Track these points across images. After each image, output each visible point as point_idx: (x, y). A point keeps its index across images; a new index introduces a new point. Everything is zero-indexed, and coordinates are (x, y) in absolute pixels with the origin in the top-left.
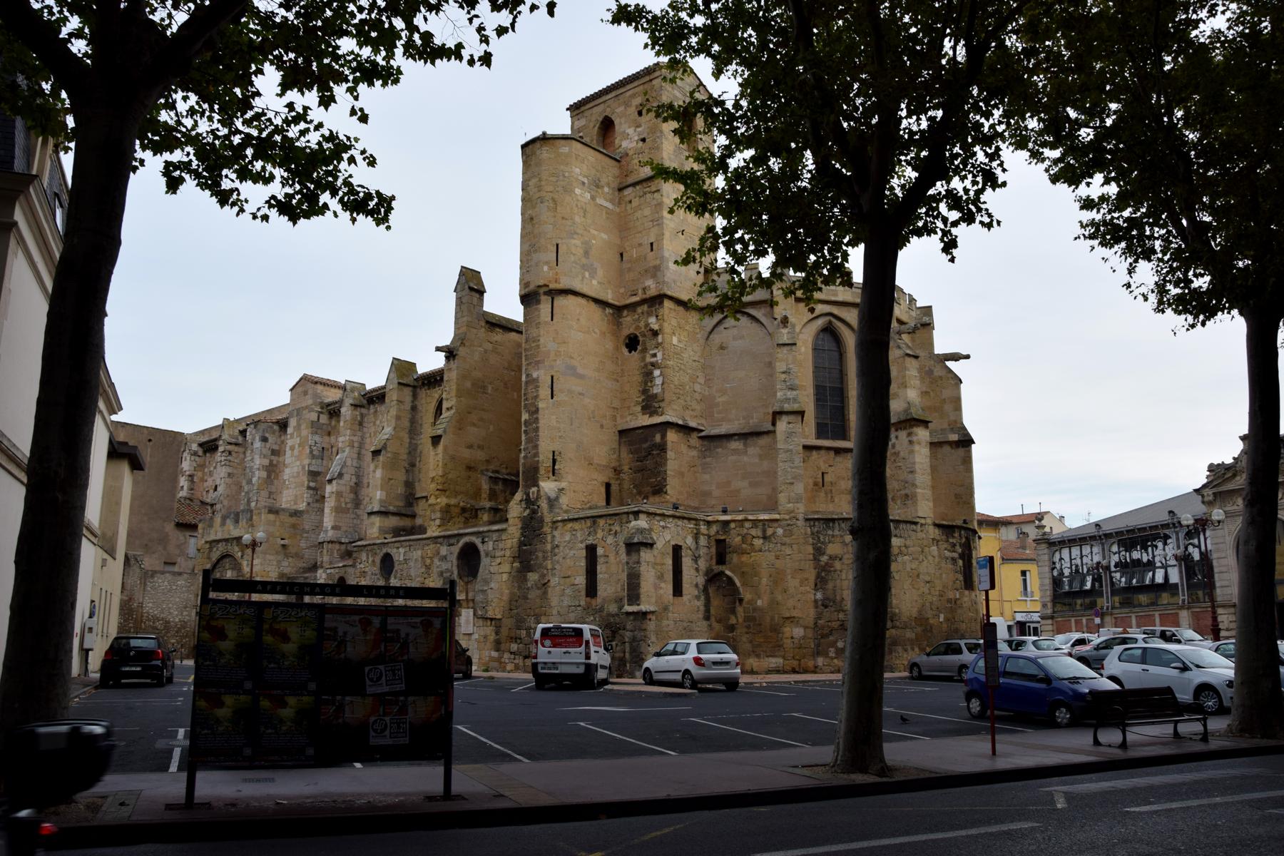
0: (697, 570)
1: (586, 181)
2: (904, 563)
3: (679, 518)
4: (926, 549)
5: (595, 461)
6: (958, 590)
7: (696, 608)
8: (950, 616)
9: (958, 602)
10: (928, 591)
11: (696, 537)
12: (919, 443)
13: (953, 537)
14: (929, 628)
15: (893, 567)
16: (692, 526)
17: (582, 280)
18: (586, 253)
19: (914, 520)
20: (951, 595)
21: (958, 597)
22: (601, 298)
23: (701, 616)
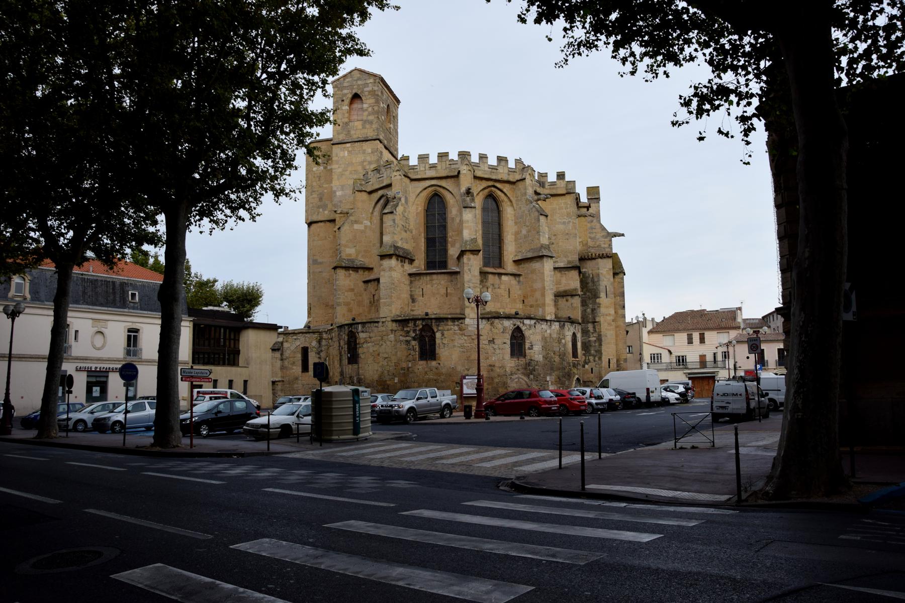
2: (368, 347)
3: (309, 333)
5: (330, 304)
8: (403, 379)
9: (410, 369)
11: (319, 342)
12: (384, 270)
13: (408, 327)
14: (386, 387)
15: (360, 351)
17: (318, 214)
18: (321, 199)
19: (376, 320)
20: (404, 365)
21: (410, 366)
22: (331, 219)
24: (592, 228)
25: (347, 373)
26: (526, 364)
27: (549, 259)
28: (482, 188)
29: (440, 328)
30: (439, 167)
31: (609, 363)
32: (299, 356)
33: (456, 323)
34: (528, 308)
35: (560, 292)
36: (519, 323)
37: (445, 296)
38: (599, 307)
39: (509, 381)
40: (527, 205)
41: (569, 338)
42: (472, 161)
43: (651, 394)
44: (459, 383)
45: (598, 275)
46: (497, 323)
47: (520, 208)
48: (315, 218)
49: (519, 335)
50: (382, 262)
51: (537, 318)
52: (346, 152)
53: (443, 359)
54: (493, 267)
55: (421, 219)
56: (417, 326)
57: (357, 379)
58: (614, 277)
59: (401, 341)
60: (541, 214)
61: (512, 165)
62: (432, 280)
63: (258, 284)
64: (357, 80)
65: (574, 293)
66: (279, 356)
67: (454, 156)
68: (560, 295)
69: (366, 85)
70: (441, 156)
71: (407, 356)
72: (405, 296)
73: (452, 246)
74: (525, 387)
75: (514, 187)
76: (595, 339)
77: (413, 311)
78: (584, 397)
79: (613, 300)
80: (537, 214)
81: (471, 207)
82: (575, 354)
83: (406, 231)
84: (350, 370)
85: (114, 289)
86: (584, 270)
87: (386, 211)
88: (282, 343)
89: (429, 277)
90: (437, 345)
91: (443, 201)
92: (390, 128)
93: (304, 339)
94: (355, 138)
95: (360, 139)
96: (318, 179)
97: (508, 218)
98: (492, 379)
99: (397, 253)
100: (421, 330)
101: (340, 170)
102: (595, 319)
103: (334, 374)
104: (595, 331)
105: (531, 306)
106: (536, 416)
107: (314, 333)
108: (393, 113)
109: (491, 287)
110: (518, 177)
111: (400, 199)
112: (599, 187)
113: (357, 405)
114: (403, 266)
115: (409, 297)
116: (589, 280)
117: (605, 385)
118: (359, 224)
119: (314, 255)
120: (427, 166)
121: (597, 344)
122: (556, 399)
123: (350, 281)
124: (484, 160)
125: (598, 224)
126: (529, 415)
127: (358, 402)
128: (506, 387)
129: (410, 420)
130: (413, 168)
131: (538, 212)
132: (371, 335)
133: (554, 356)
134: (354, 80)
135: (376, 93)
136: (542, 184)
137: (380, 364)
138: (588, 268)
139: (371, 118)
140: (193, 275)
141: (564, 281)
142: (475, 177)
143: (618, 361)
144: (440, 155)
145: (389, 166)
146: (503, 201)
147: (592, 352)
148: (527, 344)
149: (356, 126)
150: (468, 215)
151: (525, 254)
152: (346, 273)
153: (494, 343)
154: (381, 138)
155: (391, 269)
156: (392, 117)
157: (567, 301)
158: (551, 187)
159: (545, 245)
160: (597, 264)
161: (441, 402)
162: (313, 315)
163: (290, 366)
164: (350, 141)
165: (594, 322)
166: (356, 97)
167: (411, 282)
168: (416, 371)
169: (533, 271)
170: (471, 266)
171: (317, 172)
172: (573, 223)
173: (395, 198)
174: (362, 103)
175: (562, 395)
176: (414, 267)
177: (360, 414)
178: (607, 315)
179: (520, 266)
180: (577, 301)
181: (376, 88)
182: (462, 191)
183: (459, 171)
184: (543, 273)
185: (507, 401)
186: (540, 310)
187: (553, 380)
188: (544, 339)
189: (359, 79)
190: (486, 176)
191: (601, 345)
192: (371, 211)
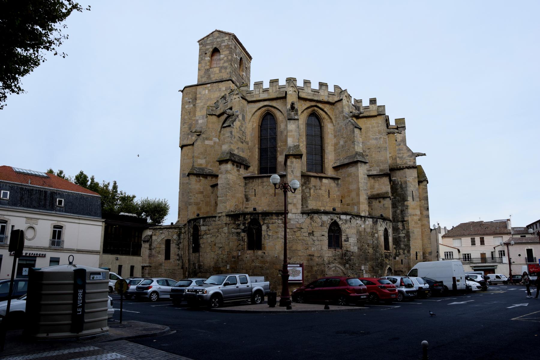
0: (179, 248)
1: (191, 100)
4: (221, 230)
6: (240, 251)
7: (177, 264)
8: (234, 266)
9: (240, 258)
10: (221, 253)
11: (179, 235)
13: (239, 220)
15: (201, 241)
16: (177, 231)
17: (188, 139)
20: (235, 254)
21: (240, 254)
23: (180, 267)
24: (400, 150)
25: (192, 260)
26: (342, 255)
27: (363, 164)
28: (306, 107)
29: (266, 222)
30: (270, 91)
31: (417, 255)
32: (163, 246)
33: (280, 217)
34: (346, 206)
35: (374, 195)
36: (336, 218)
37: (273, 195)
38: (407, 209)
39: (327, 270)
40: (344, 120)
41: (381, 233)
42: (297, 85)
43: (457, 283)
44: (281, 270)
45: (406, 182)
46: (316, 218)
47: (338, 124)
48: (185, 143)
49: (336, 228)
50: (220, 166)
51: (352, 213)
52: (207, 91)
53: (267, 248)
54: (316, 172)
55: (256, 133)
56: (246, 220)
57: (198, 265)
58: (419, 184)
59: (233, 233)
60: (356, 127)
61: (331, 89)
62: (262, 182)
63: (166, 200)
64: (216, 39)
65: (386, 196)
66: (148, 246)
67: (282, 82)
68: (372, 198)
69: (223, 41)
70: (272, 82)
71: (238, 246)
72: (240, 195)
73: (280, 155)
74: (342, 274)
75: (334, 107)
76: (404, 235)
77: (246, 208)
78: (395, 285)
79: (419, 203)
80: (352, 127)
81: (295, 119)
82: (387, 247)
83: (242, 143)
84: (194, 258)
85: (45, 196)
86: (394, 179)
87: (225, 125)
88: (151, 236)
89: (260, 180)
90: (263, 237)
91: (274, 119)
92: (243, 75)
93: (167, 233)
94: (214, 80)
95: (217, 81)
96: (188, 114)
97: (328, 132)
98: (312, 267)
99: (233, 158)
100: (249, 223)
101: (202, 104)
102: (404, 219)
103: (185, 261)
104: (404, 228)
105: (348, 205)
106: (344, 305)
107: (175, 228)
108: (246, 64)
109: (313, 188)
110: (336, 99)
111: (238, 116)
112: (404, 118)
113: (80, 292)
114: (238, 171)
115: (244, 196)
116: (398, 187)
117: (414, 273)
118: (210, 140)
119: (183, 170)
120: (261, 90)
121: (406, 240)
122: (366, 287)
123: (200, 186)
124: (308, 85)
125: (405, 147)
126: (336, 303)
127: (83, 287)
128: (324, 275)
129: (215, 305)
130: (250, 92)
131: (353, 125)
132: (210, 227)
133: (367, 248)
134: (215, 39)
135: (230, 46)
136: (357, 108)
137: (216, 253)
138: (398, 177)
139: (226, 65)
140: (119, 192)
141: (377, 186)
142: (300, 98)
143: (424, 254)
144: (272, 81)
145: (232, 93)
146: (324, 119)
147: (402, 246)
148: (343, 236)
149: (215, 71)
150: (292, 126)
151: (342, 161)
152: (196, 178)
153: (313, 235)
154: (234, 79)
155: (227, 172)
156: (245, 68)
157: (380, 202)
158: (365, 110)
159: (360, 152)
160: (405, 173)
161: (252, 288)
162: (181, 216)
163: (156, 254)
164: (210, 82)
165: (403, 221)
166: (216, 51)
167: (246, 184)
168: (245, 259)
169: (349, 175)
170: (294, 168)
171: (188, 108)
172: (384, 138)
173: (233, 115)
174: (220, 55)
175: (373, 284)
176: (249, 172)
177: (84, 303)
178: (413, 215)
179: (339, 172)
180: (388, 203)
181: (230, 43)
182: (287, 108)
183: (286, 92)
184: (358, 176)
185: (316, 289)
186: (356, 207)
187: (367, 269)
188: (359, 233)
189: (218, 37)
190: (309, 97)
191: (410, 240)
192: (219, 131)
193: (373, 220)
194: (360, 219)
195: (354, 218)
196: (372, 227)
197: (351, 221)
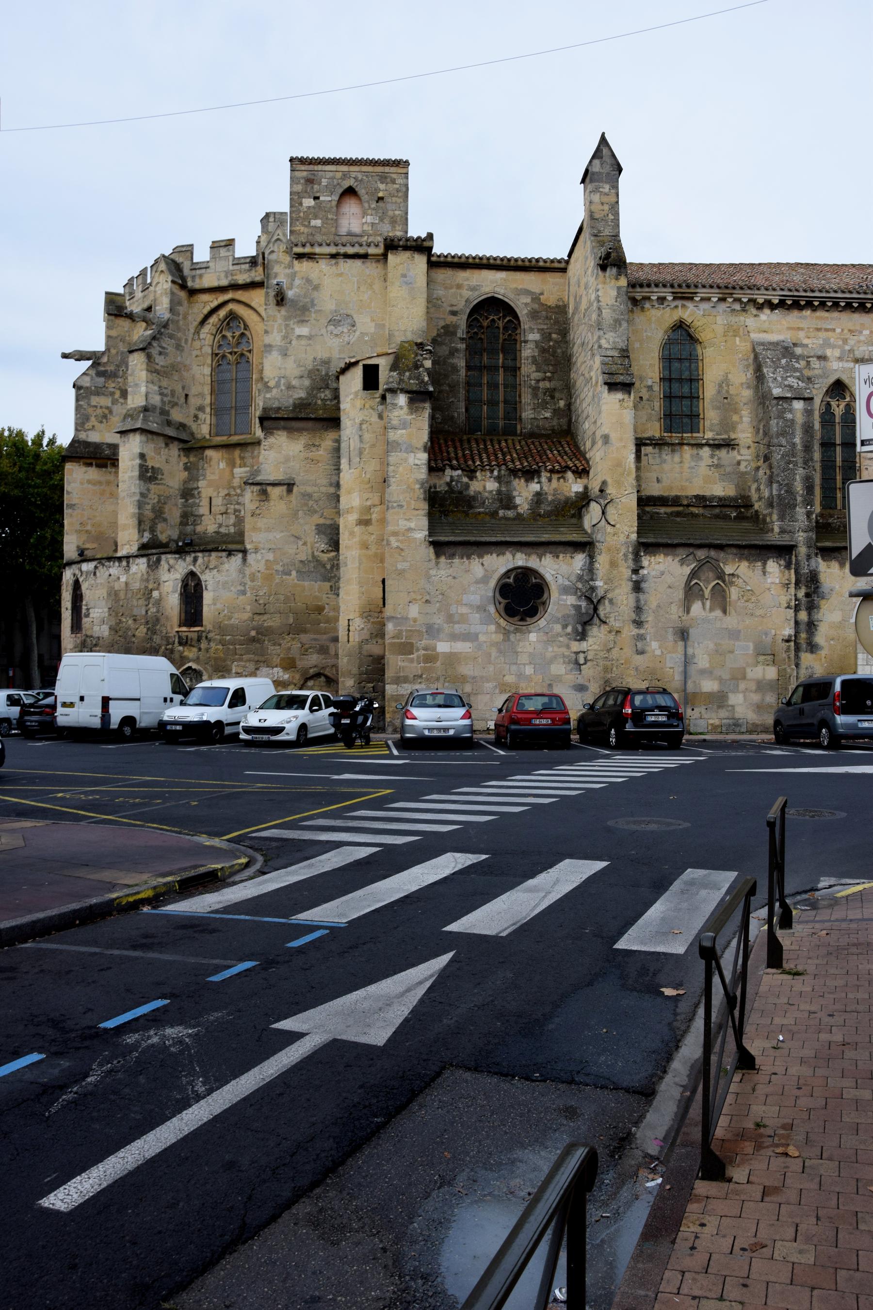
133: (132, 626)
188: (113, 594)
193: (149, 560)
194: (117, 564)
195: (103, 565)
196: (145, 576)
197: (98, 574)
